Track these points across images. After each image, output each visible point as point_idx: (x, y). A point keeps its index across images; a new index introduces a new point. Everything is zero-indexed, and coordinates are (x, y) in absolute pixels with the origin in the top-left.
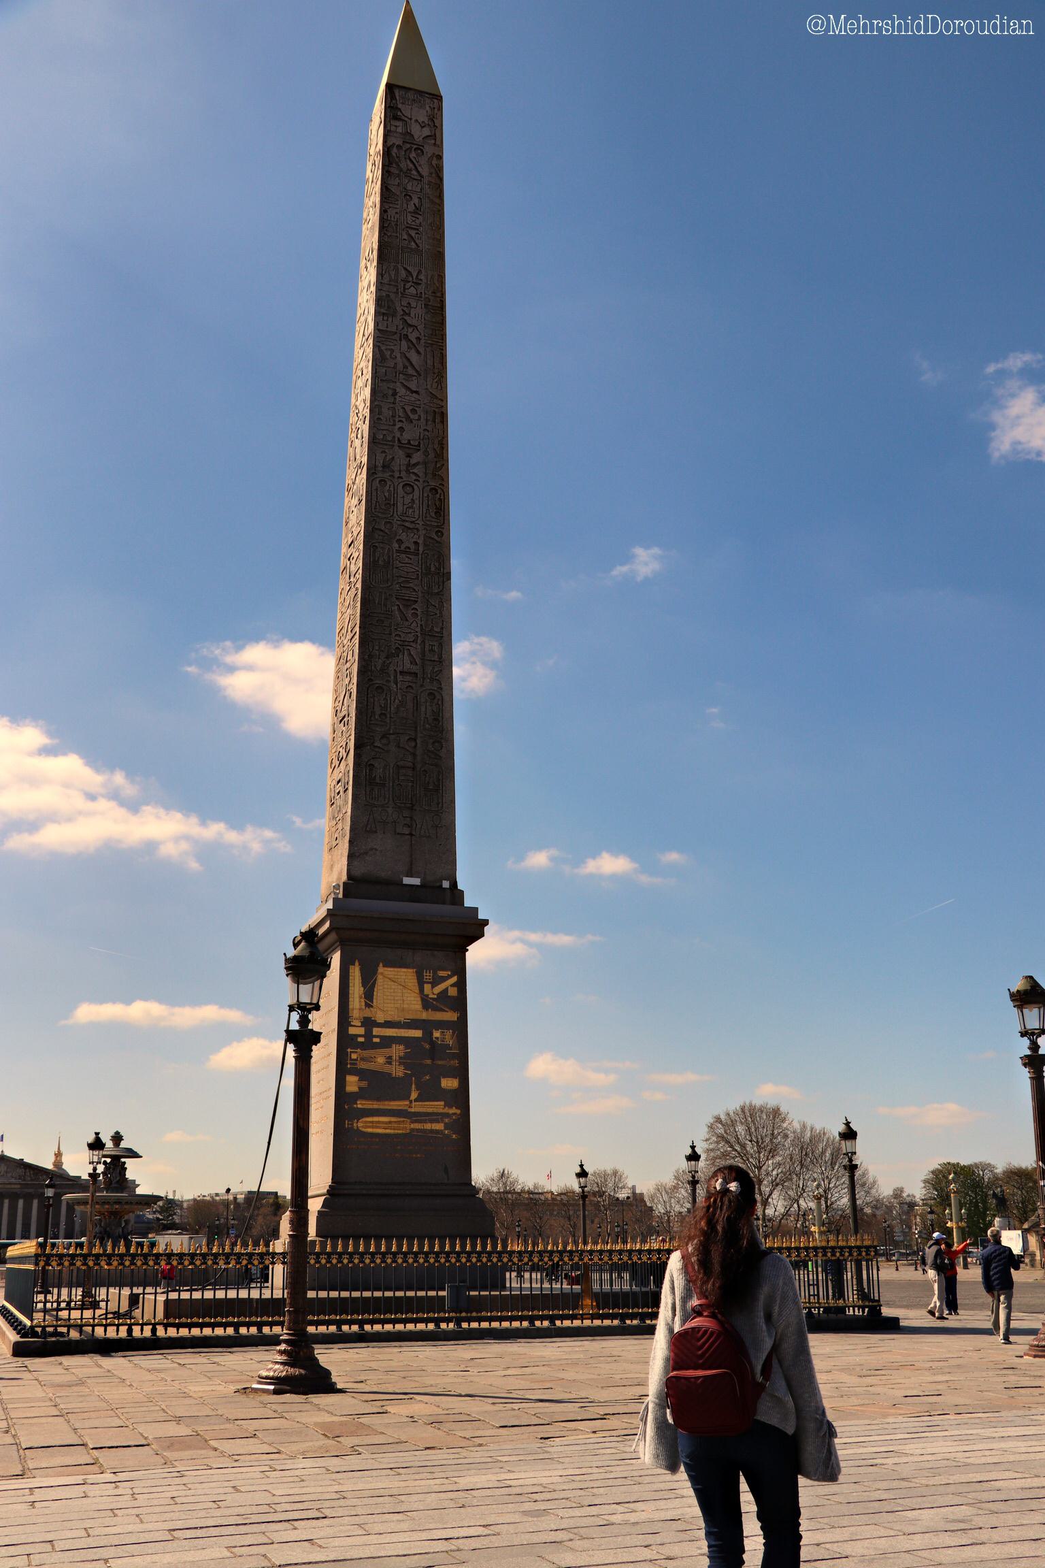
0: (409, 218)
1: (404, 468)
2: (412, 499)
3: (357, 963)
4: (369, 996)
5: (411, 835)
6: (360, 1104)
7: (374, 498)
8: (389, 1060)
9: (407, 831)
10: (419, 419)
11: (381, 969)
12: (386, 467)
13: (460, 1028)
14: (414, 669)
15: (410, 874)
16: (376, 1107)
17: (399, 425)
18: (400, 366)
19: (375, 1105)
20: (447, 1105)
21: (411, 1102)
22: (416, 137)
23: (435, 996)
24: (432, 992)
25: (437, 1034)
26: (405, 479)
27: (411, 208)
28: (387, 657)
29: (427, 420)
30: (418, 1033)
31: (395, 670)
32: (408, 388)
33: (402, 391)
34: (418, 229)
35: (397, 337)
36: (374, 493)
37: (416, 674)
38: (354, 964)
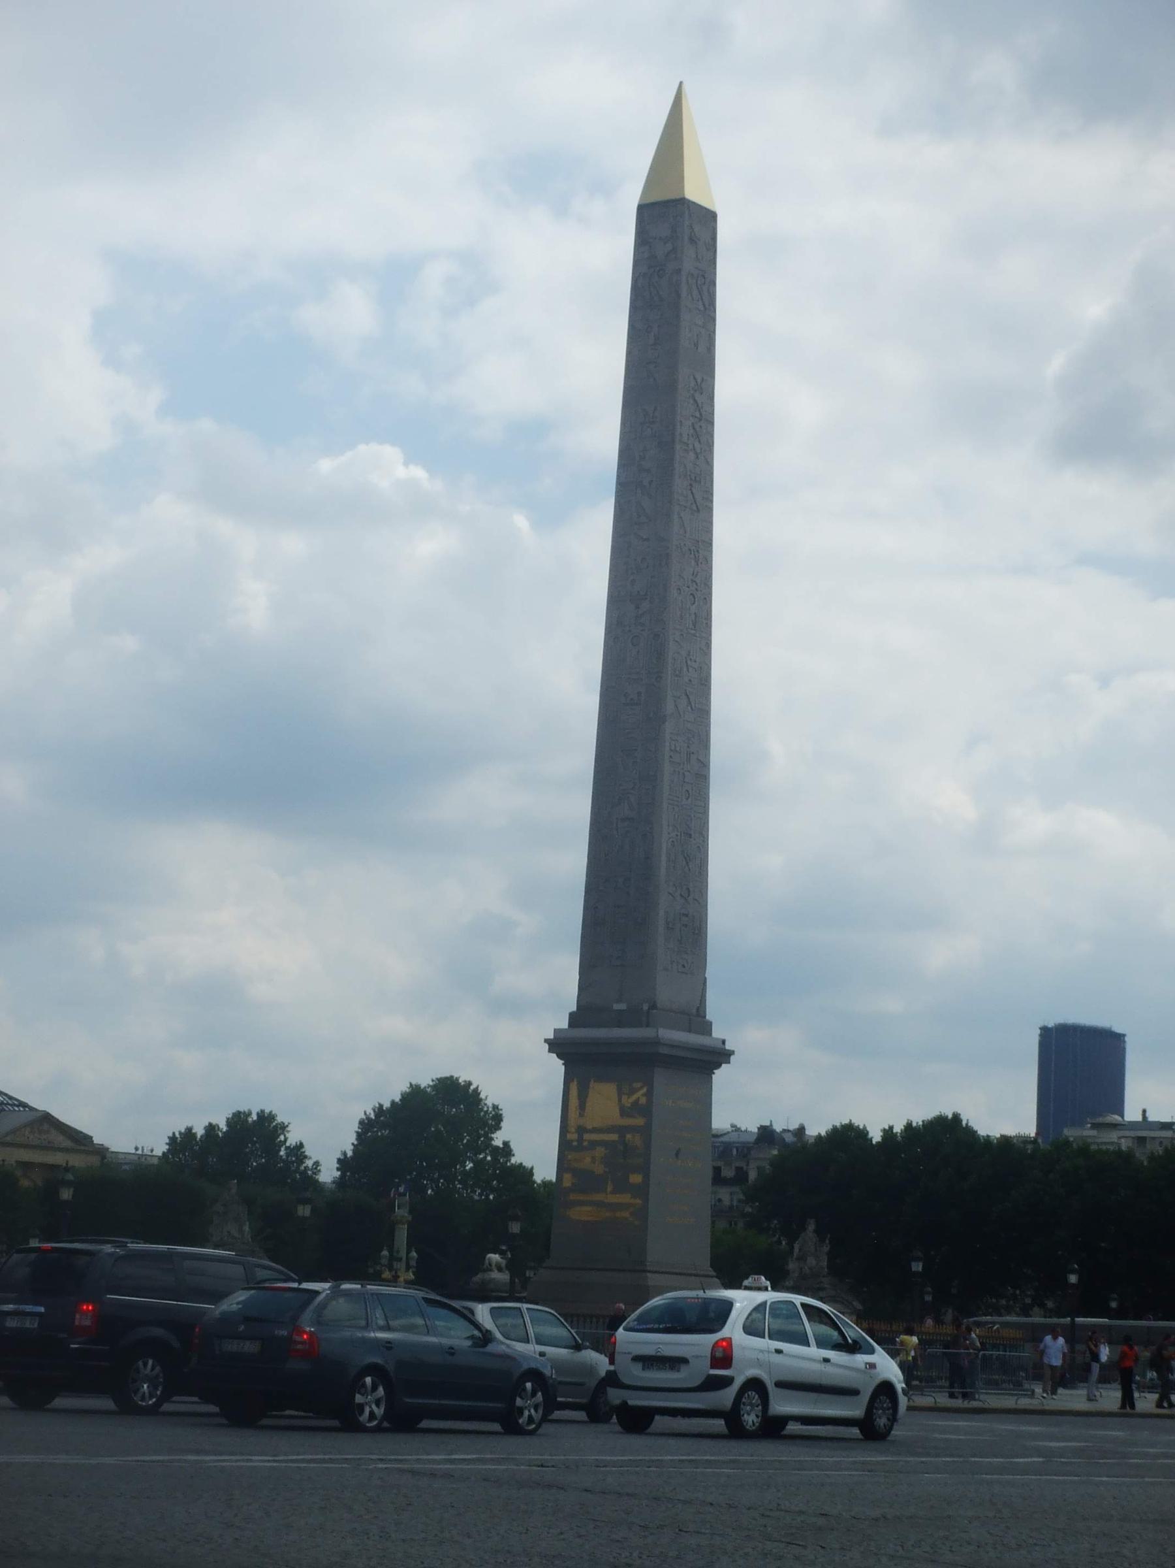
2: (638, 652)
3: (575, 1080)
4: (582, 1106)
6: (572, 1197)
8: (593, 1159)
11: (592, 1084)
13: (646, 1132)
15: (619, 1001)
16: (582, 1198)
17: (632, 578)
19: (582, 1197)
21: (607, 1194)
23: (629, 1105)
24: (627, 1101)
25: (629, 1136)
30: (614, 1137)
31: (617, 818)
38: (573, 1080)
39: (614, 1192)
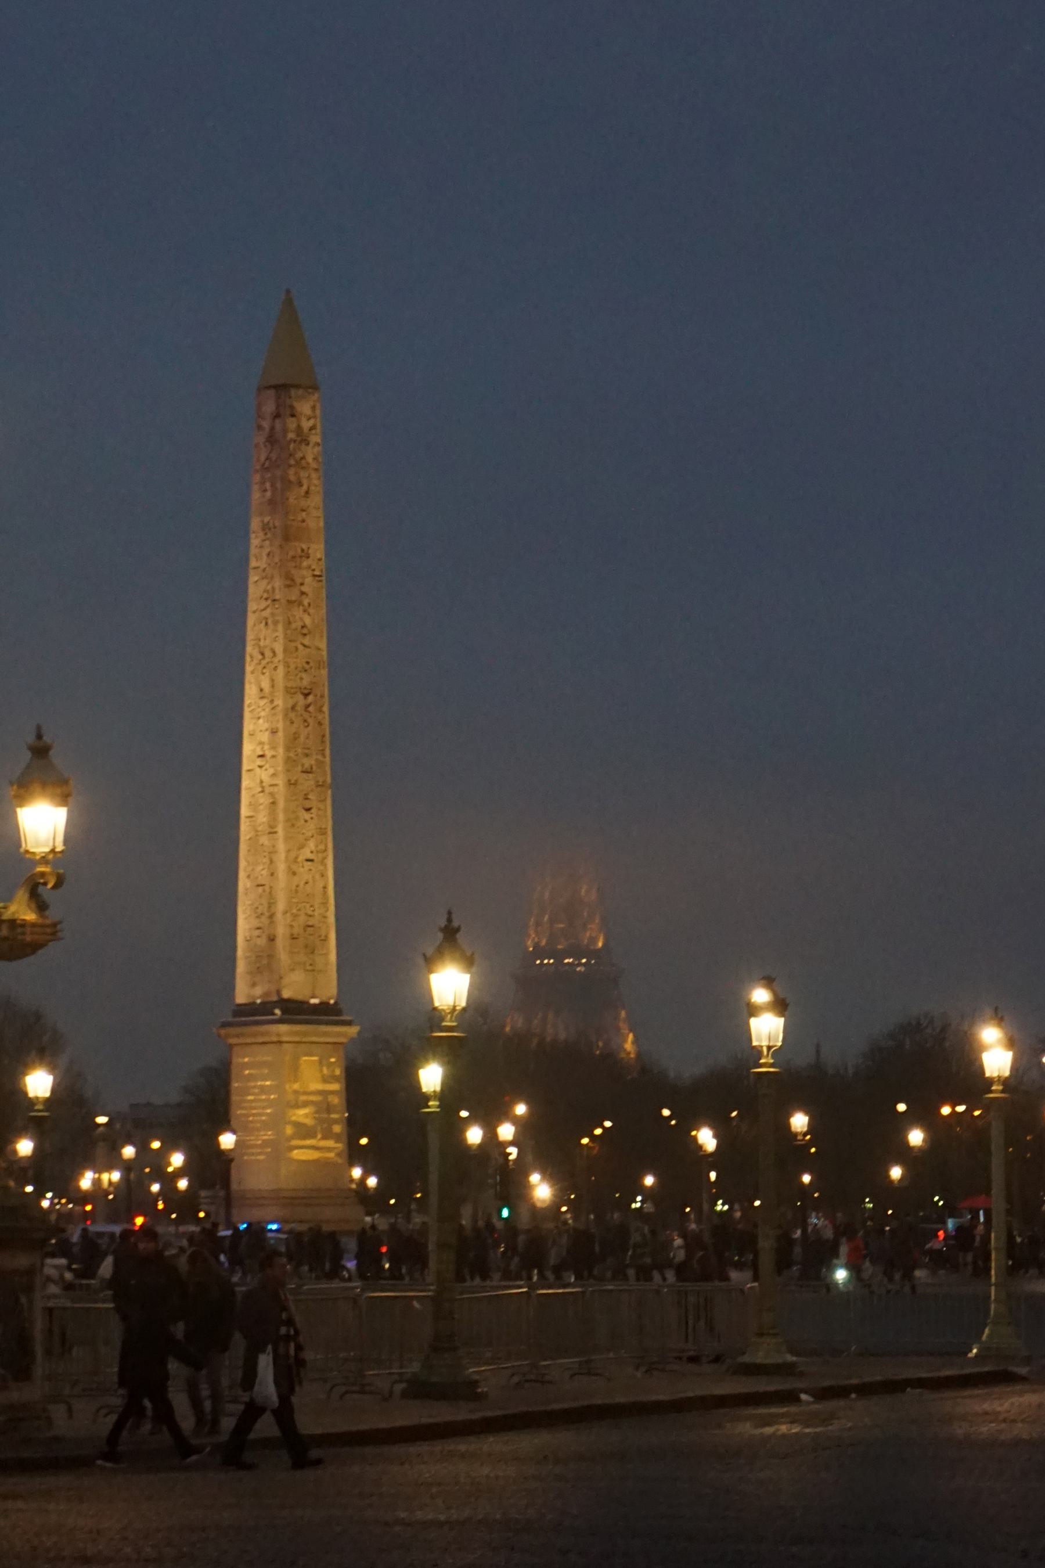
12: (293, 708)
15: (313, 997)
30: (318, 1098)
32: (305, 646)
33: (301, 647)
37: (312, 860)
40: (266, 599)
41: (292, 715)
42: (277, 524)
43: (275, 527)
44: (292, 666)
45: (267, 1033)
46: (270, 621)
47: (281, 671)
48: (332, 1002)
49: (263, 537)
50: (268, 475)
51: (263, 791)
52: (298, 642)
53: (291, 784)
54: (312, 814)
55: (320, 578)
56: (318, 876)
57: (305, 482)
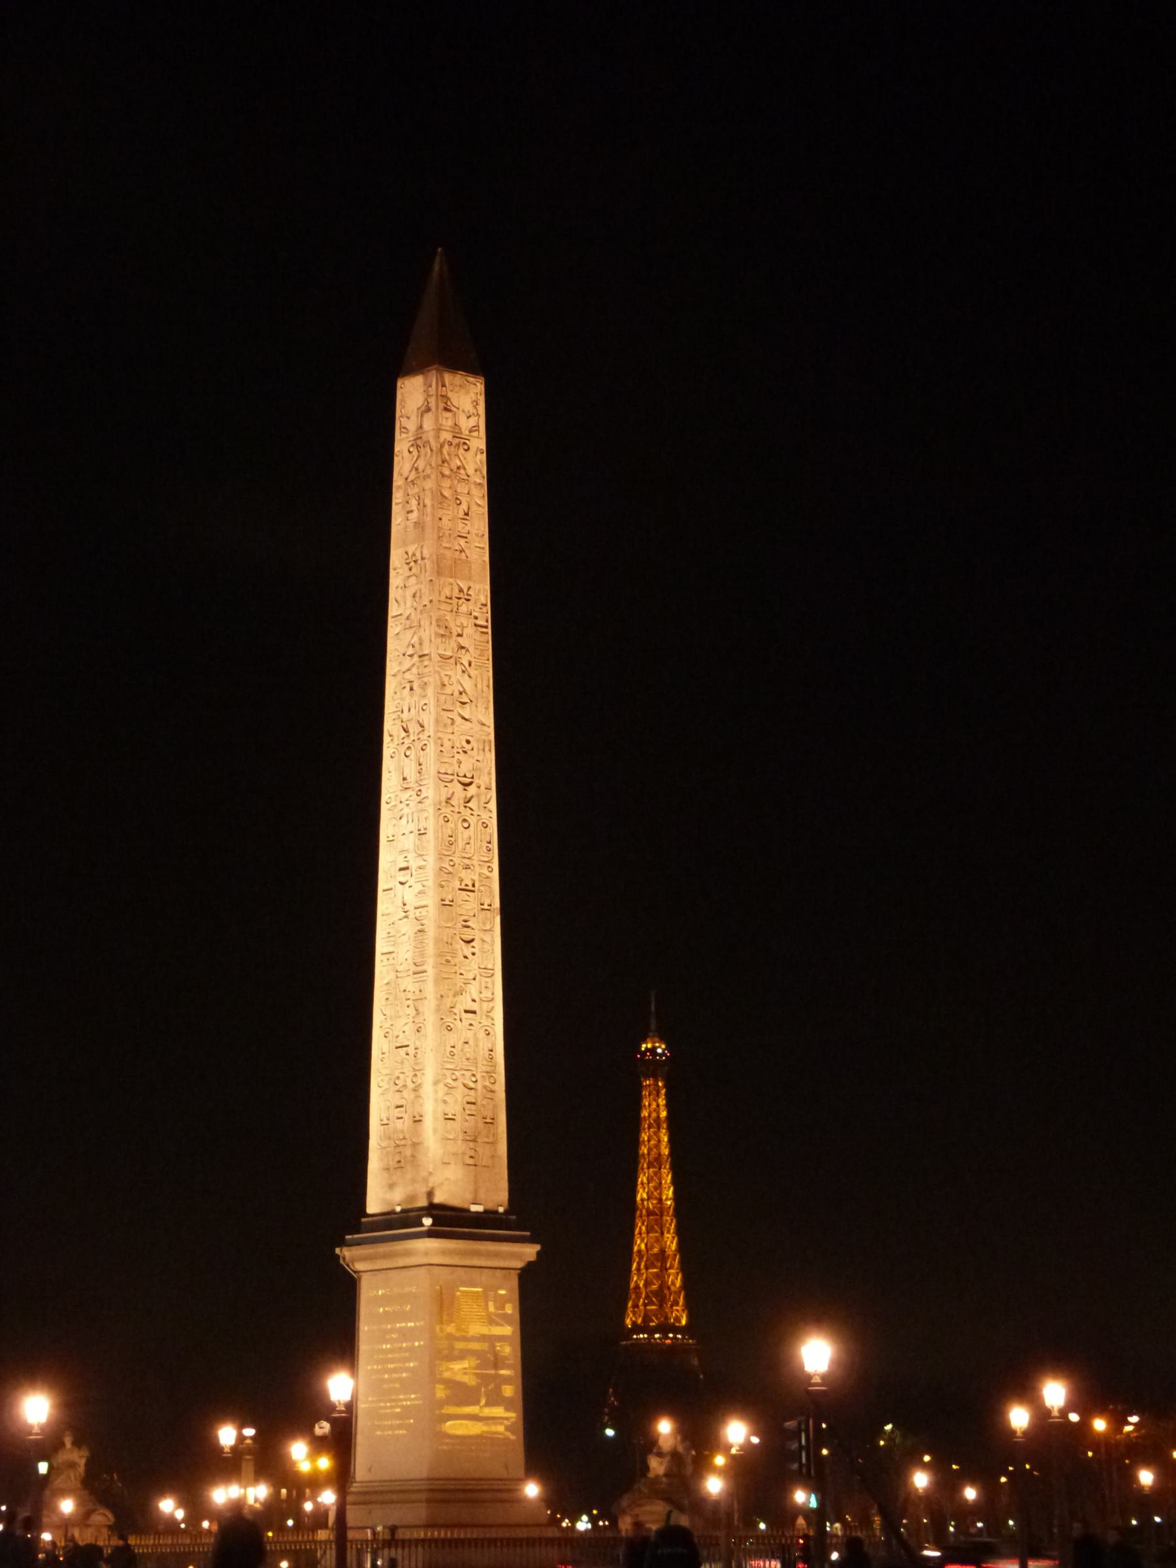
0: (461, 525)
1: (462, 802)
5: (475, 1165)
7: (440, 834)
9: (471, 1161)
10: (472, 749)
14: (474, 1007)
18: (456, 694)
20: (507, 1409)
22: (463, 430)
26: (463, 814)
27: (461, 514)
28: (454, 996)
29: (478, 749)
30: (485, 1346)
33: (459, 720)
34: (466, 538)
35: (452, 660)
36: (440, 830)
39: (488, 1404)
40: (411, 656)
41: (447, 810)
42: (426, 553)
43: (423, 559)
44: (447, 744)
45: (408, 1253)
46: (415, 687)
47: (431, 749)
48: (501, 1210)
49: (408, 573)
50: (414, 491)
51: (406, 917)
52: (455, 713)
53: (445, 904)
54: (473, 947)
55: (484, 630)
56: (482, 1034)
57: (464, 499)
